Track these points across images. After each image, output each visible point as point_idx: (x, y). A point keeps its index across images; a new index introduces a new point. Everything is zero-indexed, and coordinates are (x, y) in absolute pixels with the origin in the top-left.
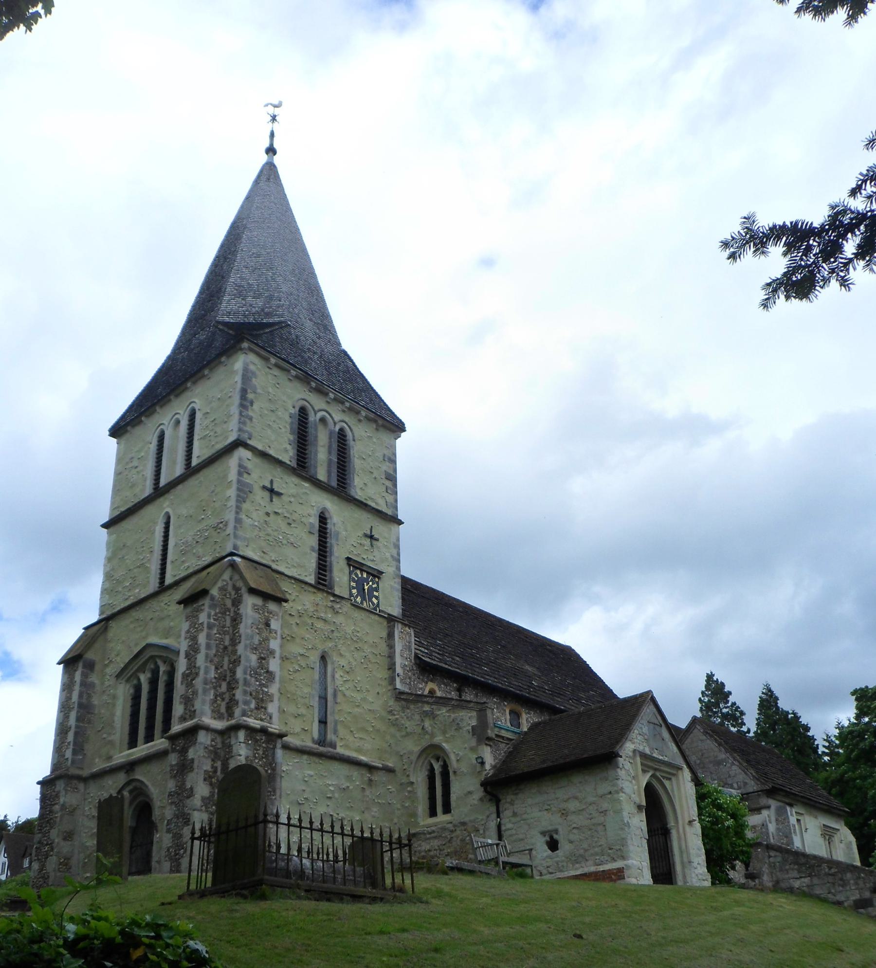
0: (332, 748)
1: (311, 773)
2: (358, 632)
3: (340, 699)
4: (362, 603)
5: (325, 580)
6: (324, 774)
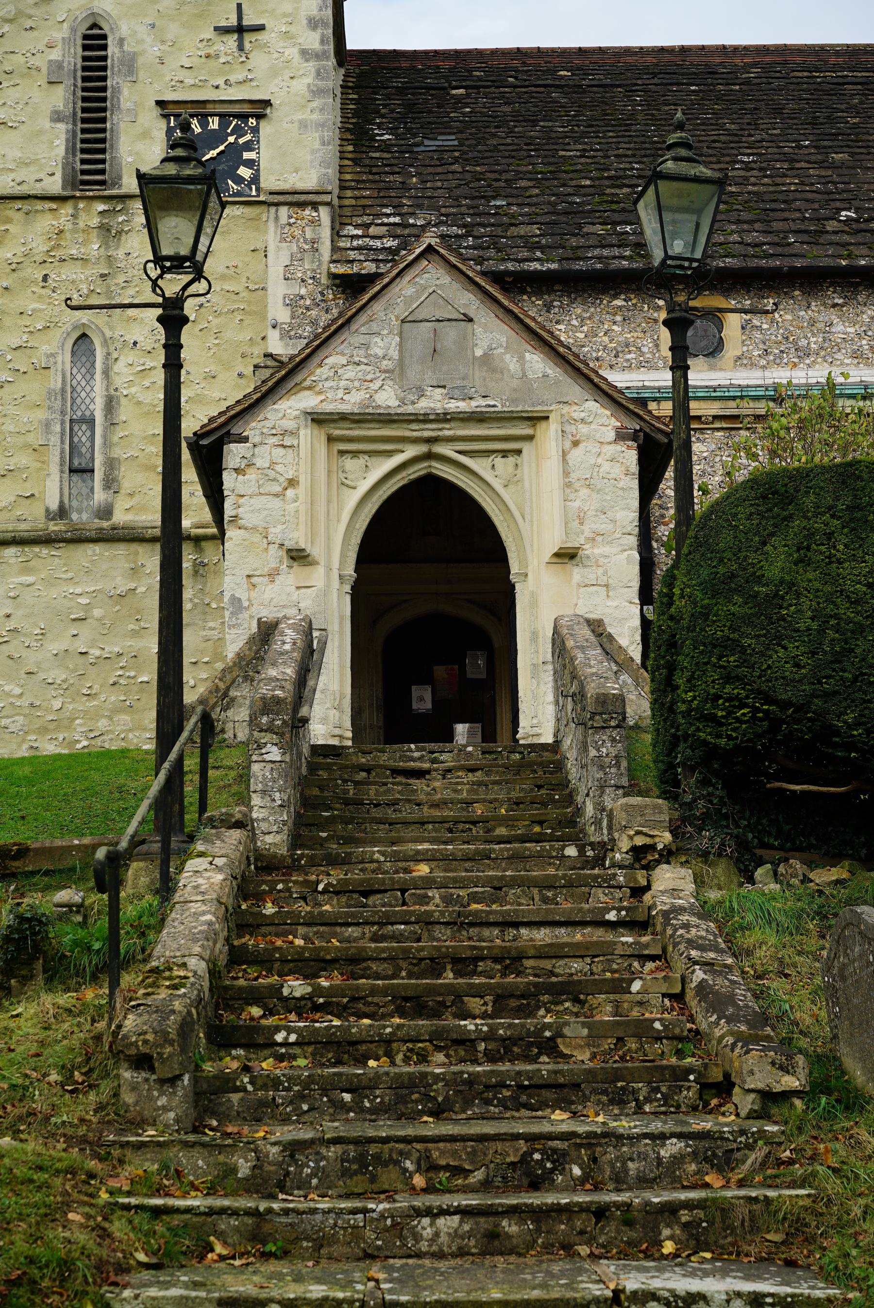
3: (124, 413)
5: (102, 172)
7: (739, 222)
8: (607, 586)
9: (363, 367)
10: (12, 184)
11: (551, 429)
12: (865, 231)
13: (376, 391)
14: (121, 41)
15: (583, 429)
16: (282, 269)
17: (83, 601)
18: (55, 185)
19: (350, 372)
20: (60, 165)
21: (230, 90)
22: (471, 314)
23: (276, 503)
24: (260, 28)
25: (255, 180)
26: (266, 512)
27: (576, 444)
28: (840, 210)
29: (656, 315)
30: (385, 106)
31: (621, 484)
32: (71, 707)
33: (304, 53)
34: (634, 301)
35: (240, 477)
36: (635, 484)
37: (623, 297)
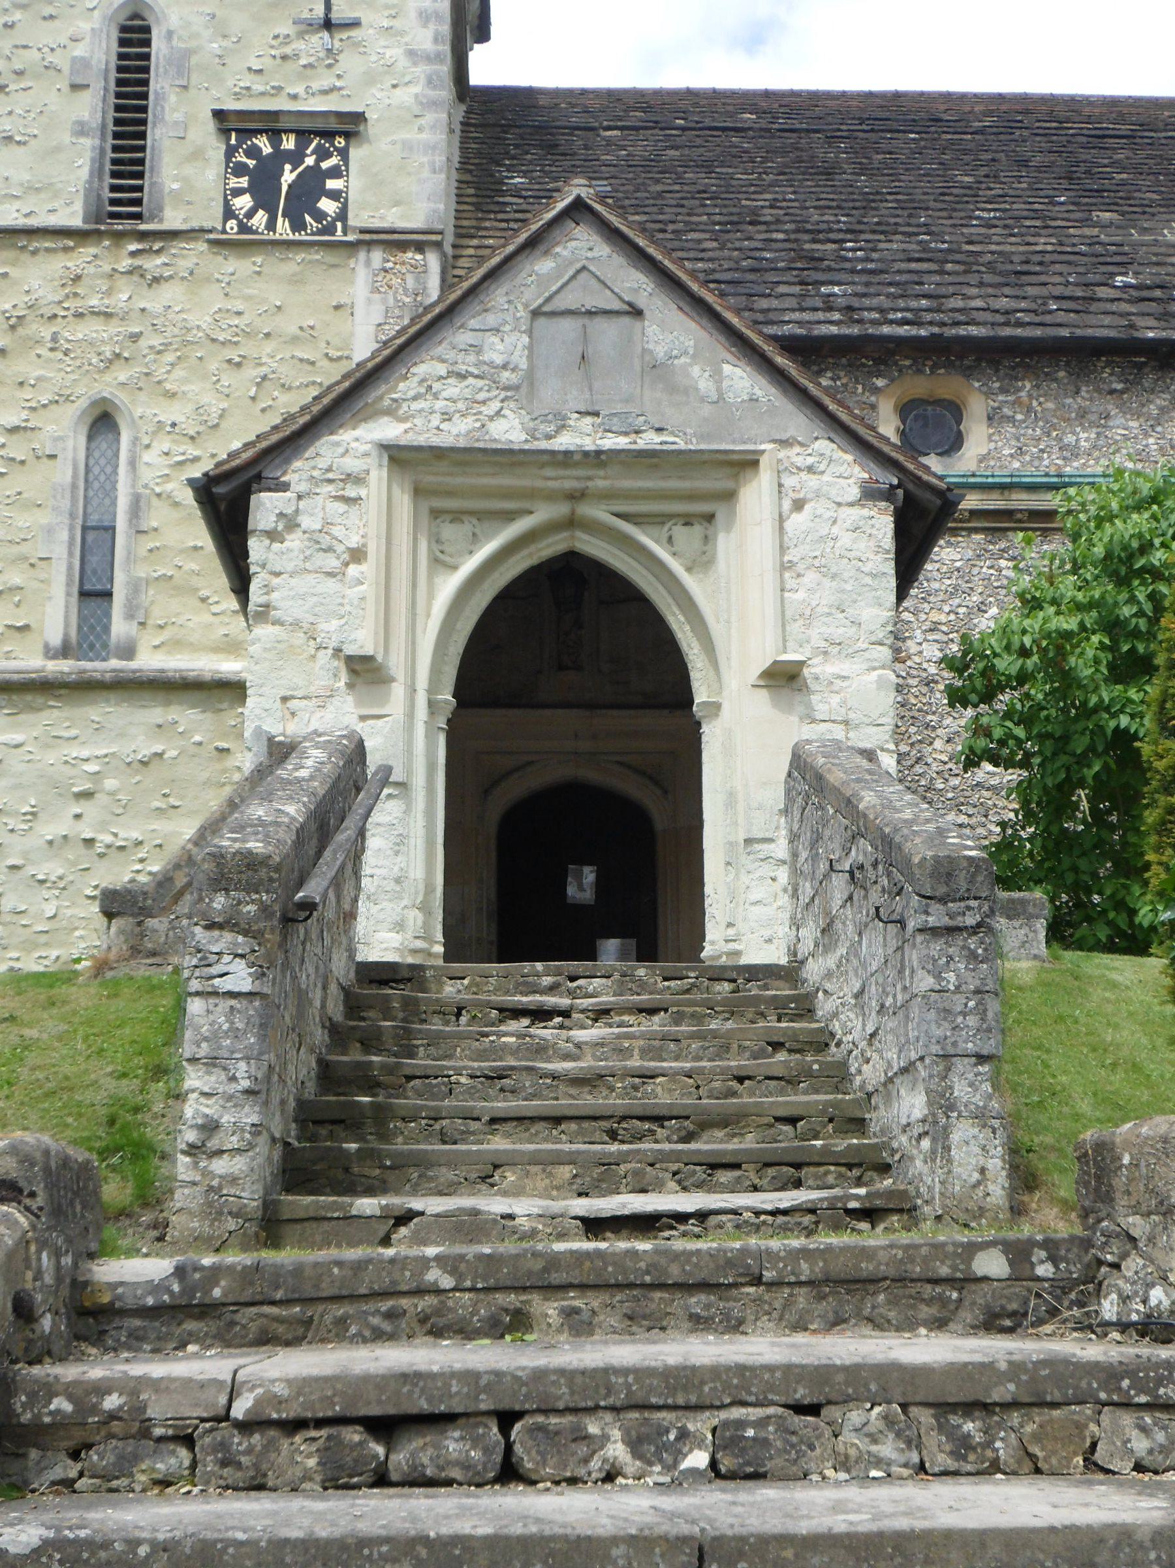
0: (121, 658)
1: (18, 738)
2: (239, 313)
4: (271, 225)
6: (66, 734)
7: (981, 284)
8: (846, 723)
9: (471, 380)
10: (16, 215)
11: (765, 478)
12: (1149, 300)
13: (491, 418)
14: (170, 34)
15: (812, 482)
16: (372, 329)
17: (92, 767)
18: (73, 216)
19: (453, 388)
20: (82, 192)
21: (312, 101)
22: (641, 302)
23: (331, 585)
24: (355, 24)
25: (342, 215)
26: (315, 599)
27: (799, 505)
28: (1113, 275)
29: (873, 399)
30: (516, 146)
31: (868, 568)
32: (69, 912)
33: (411, 53)
34: (844, 381)
35: (276, 546)
36: (890, 568)
37: (829, 374)
